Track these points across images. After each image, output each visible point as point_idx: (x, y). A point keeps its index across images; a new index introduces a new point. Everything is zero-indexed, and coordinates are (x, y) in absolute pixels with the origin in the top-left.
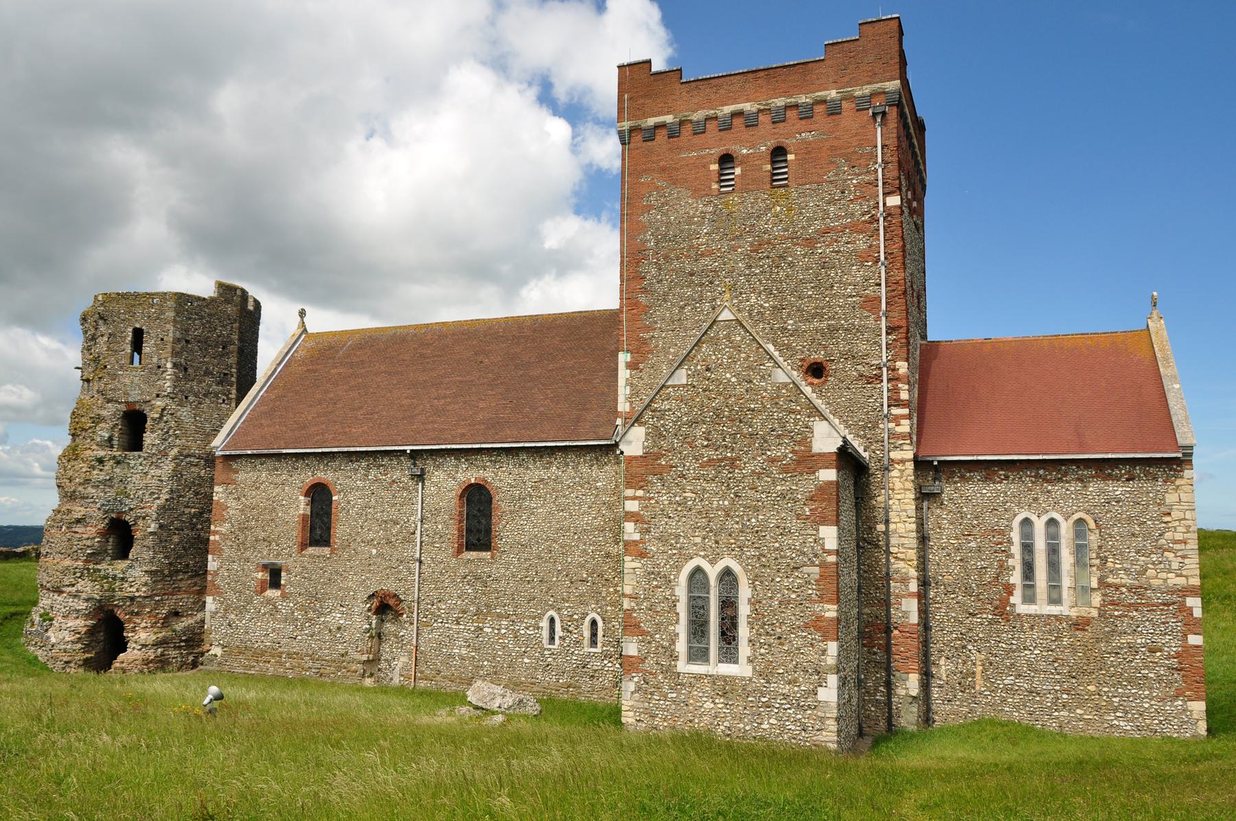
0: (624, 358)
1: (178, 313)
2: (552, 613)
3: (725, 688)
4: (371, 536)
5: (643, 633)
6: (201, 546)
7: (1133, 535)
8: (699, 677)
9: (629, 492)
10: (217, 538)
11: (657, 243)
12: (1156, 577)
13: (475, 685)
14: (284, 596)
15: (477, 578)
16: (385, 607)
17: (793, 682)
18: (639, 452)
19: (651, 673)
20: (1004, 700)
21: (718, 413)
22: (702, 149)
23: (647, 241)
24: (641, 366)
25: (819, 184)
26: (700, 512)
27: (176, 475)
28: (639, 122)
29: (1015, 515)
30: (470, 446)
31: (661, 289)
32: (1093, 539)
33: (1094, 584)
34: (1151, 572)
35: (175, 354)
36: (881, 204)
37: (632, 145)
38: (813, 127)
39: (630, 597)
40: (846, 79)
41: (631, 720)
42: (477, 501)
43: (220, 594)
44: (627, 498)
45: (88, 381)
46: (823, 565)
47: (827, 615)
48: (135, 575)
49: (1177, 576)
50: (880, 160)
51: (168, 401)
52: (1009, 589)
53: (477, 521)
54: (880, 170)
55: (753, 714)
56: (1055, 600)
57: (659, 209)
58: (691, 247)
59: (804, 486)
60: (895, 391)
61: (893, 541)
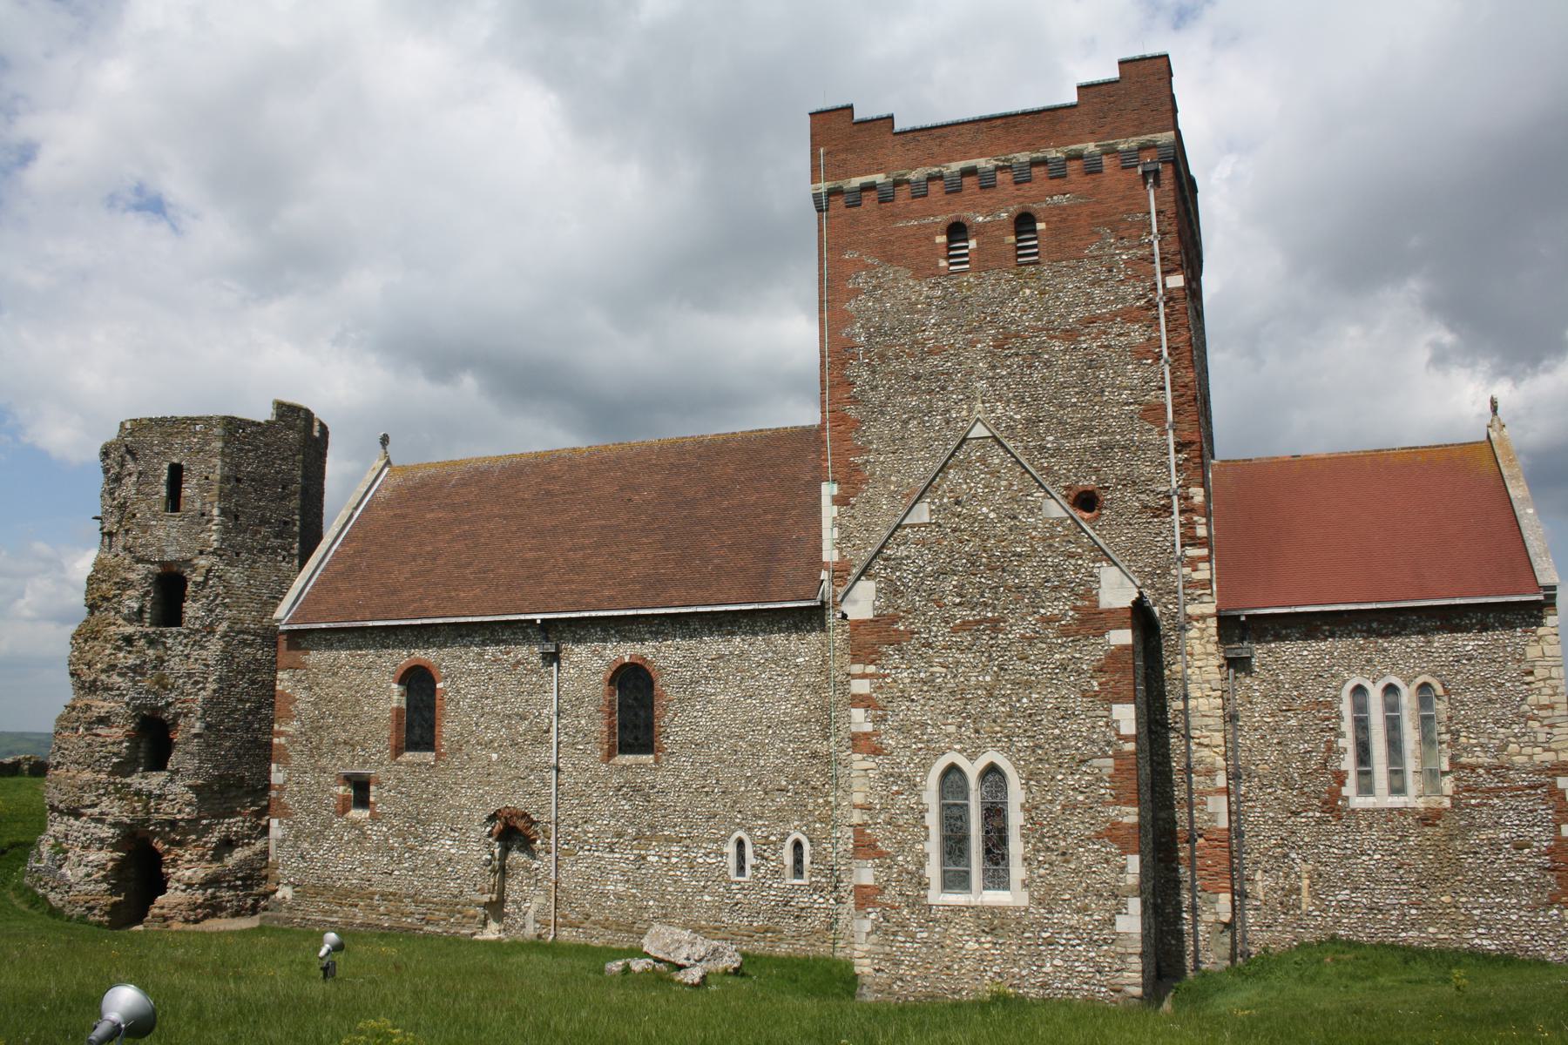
0: (828, 490)
1: (226, 443)
2: (740, 834)
3: (993, 923)
4: (490, 735)
5: (881, 855)
6: (263, 753)
7: (1490, 700)
8: (957, 910)
9: (857, 669)
11: (869, 337)
12: (1520, 754)
13: (652, 931)
14: (375, 818)
15: (637, 790)
16: (513, 833)
17: (1084, 910)
18: (869, 615)
19: (893, 908)
21: (973, 560)
22: (924, 217)
23: (855, 335)
24: (853, 501)
25: (1079, 259)
26: (952, 693)
27: (227, 657)
28: (840, 183)
29: (1345, 682)
30: (622, 613)
31: (876, 398)
32: (1441, 708)
33: (1445, 766)
34: (1513, 748)
35: (223, 496)
36: (1160, 285)
37: (831, 213)
38: (1068, 187)
39: (862, 807)
40: (1107, 129)
41: (867, 970)
43: (288, 816)
44: (855, 677)
45: (110, 534)
46: (1119, 755)
47: (1126, 820)
48: (172, 791)
49: (1545, 750)
50: (1155, 230)
51: (214, 559)
52: (1340, 778)
53: (634, 713)
54: (1156, 243)
55: (1031, 955)
56: (1398, 789)
57: (870, 294)
58: (915, 342)
59: (1091, 653)
60: (1189, 526)
61: (1194, 722)
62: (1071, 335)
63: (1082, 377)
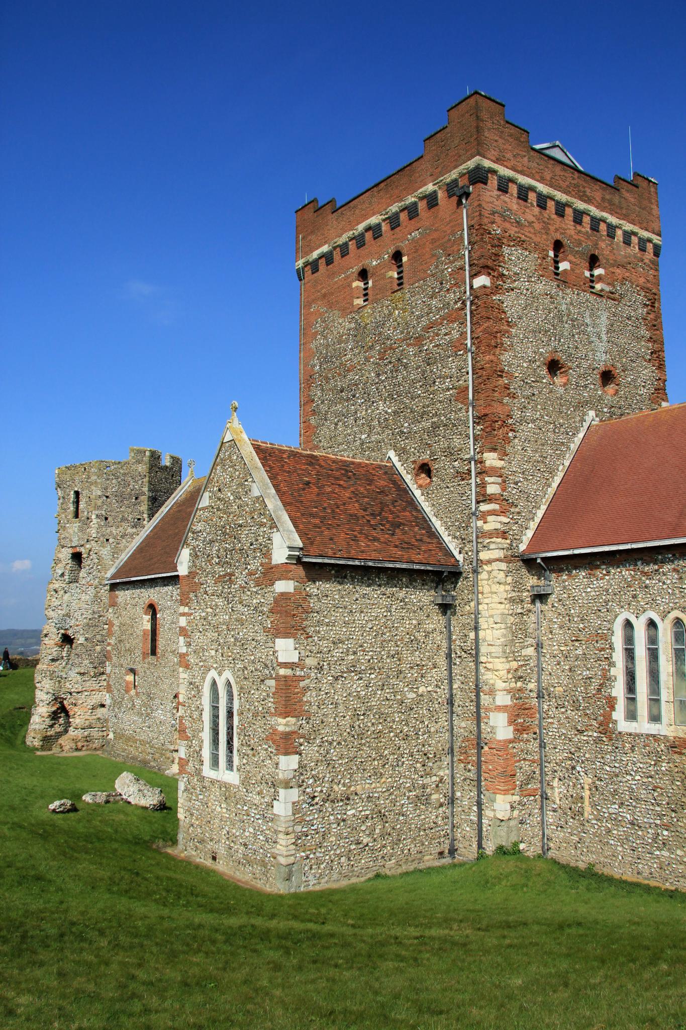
20: (609, 831)
40: (439, 169)
50: (466, 243)
52: (611, 703)
56: (655, 718)
60: (482, 486)
61: (483, 649)
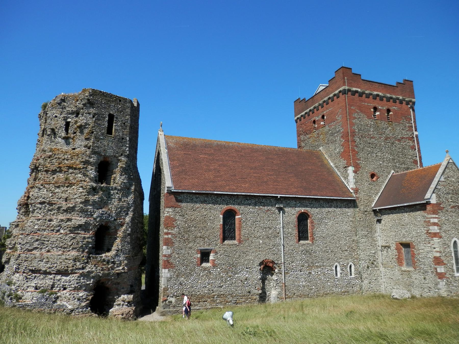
2: (336, 264)
5: (445, 264)
10: (170, 236)
24: (358, 172)
42: (303, 219)
53: (303, 228)
58: (369, 134)
62: (399, 140)
63: (402, 151)
